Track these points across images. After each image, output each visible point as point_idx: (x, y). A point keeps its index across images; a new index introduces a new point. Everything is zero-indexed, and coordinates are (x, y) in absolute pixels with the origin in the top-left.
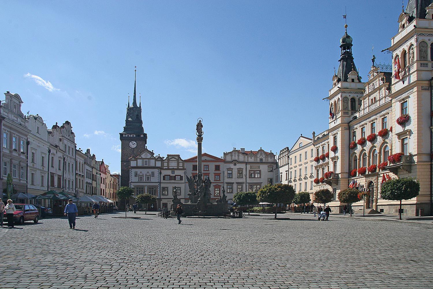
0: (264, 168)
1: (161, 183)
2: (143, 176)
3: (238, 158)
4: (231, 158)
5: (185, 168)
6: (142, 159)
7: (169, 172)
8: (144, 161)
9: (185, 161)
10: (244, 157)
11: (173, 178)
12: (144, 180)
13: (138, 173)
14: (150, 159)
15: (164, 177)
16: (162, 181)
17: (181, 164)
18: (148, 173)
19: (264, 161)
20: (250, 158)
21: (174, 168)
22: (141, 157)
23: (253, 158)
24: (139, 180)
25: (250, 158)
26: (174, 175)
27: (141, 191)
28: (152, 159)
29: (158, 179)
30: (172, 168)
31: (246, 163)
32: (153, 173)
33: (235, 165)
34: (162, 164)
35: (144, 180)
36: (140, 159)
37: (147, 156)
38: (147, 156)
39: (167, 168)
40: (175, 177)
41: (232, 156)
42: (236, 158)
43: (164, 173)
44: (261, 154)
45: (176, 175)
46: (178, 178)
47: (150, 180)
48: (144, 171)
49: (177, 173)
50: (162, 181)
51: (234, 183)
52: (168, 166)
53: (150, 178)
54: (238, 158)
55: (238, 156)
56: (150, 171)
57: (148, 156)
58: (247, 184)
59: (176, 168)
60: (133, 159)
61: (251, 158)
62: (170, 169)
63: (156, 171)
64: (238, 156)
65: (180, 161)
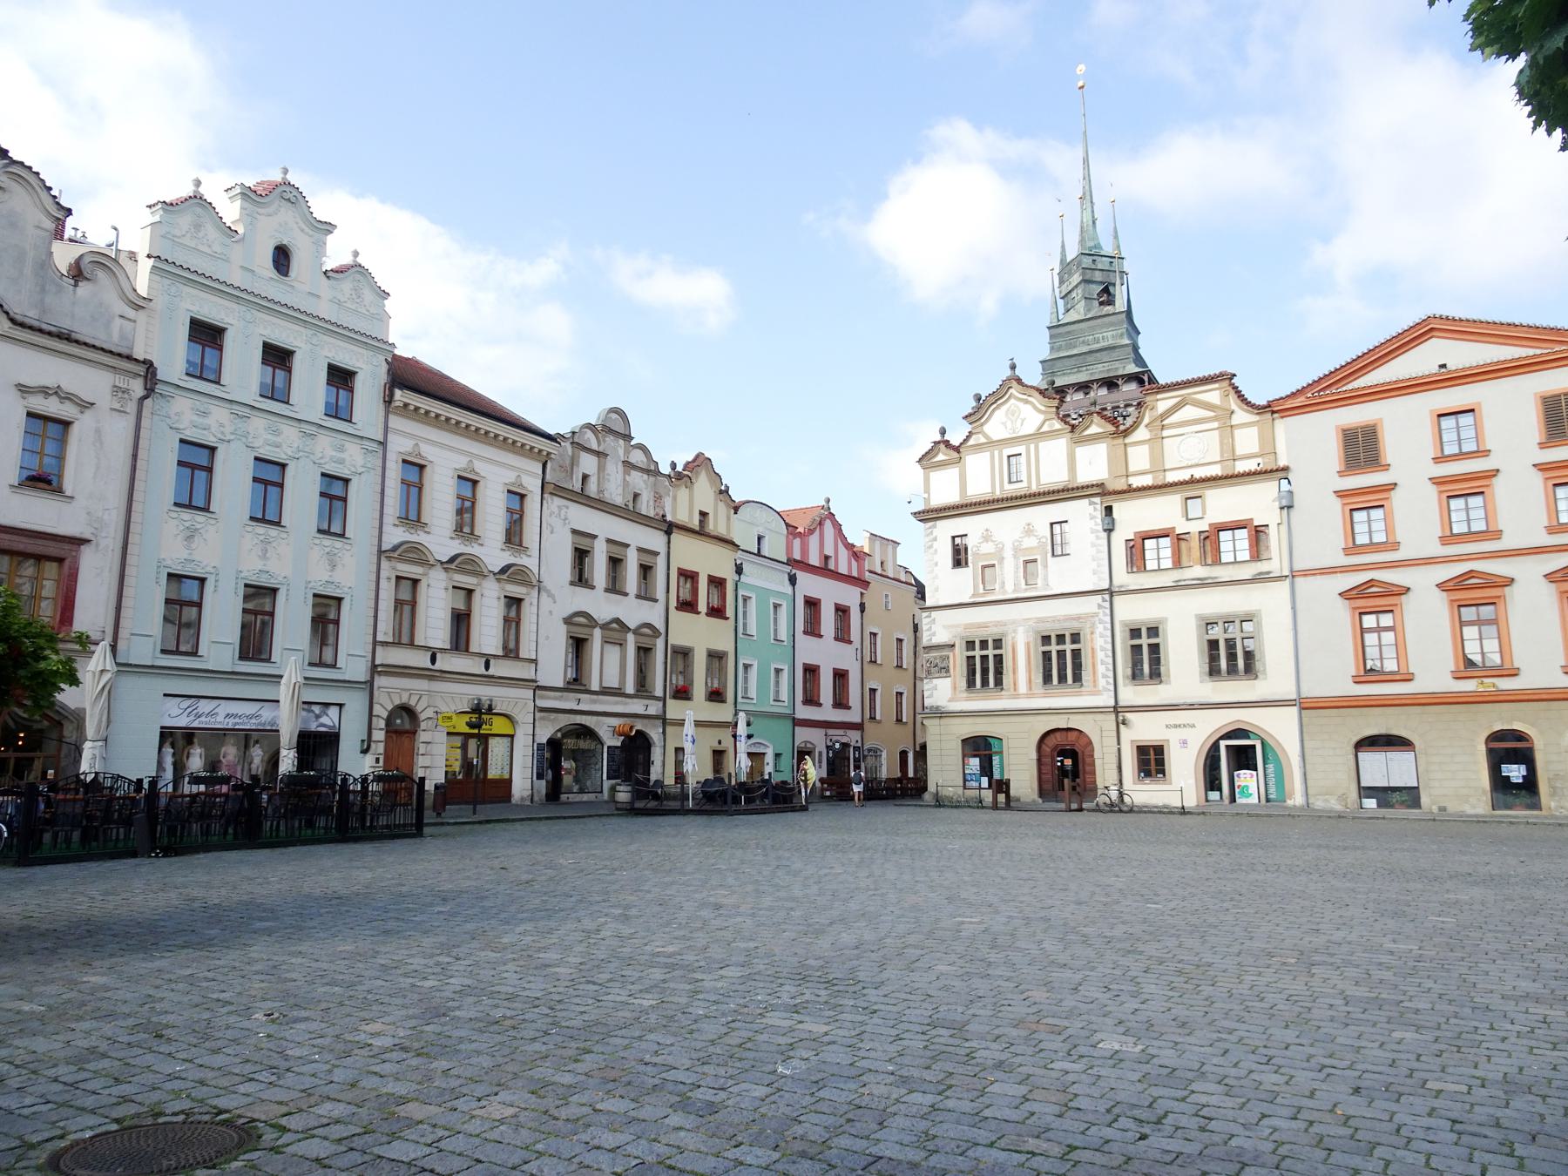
2: (1002, 559)
5: (1282, 464)
6: (991, 444)
7: (1163, 512)
8: (1005, 459)
9: (1271, 409)
12: (1009, 587)
13: (971, 542)
16: (1122, 577)
17: (1248, 440)
18: (1029, 531)
21: (1199, 473)
22: (986, 436)
24: (976, 587)
27: (1145, 650)
28: (1052, 434)
30: (1184, 475)
34: (1120, 462)
35: (1009, 587)
36: (979, 447)
37: (1019, 421)
39: (1147, 480)
40: (1211, 538)
43: (1133, 516)
46: (1235, 545)
47: (1046, 578)
48: (1006, 528)
49: (1222, 505)
50: (1122, 577)
52: (1158, 467)
53: (1046, 566)
56: (1041, 516)
60: (941, 457)
63: (1082, 516)
65: (1241, 416)
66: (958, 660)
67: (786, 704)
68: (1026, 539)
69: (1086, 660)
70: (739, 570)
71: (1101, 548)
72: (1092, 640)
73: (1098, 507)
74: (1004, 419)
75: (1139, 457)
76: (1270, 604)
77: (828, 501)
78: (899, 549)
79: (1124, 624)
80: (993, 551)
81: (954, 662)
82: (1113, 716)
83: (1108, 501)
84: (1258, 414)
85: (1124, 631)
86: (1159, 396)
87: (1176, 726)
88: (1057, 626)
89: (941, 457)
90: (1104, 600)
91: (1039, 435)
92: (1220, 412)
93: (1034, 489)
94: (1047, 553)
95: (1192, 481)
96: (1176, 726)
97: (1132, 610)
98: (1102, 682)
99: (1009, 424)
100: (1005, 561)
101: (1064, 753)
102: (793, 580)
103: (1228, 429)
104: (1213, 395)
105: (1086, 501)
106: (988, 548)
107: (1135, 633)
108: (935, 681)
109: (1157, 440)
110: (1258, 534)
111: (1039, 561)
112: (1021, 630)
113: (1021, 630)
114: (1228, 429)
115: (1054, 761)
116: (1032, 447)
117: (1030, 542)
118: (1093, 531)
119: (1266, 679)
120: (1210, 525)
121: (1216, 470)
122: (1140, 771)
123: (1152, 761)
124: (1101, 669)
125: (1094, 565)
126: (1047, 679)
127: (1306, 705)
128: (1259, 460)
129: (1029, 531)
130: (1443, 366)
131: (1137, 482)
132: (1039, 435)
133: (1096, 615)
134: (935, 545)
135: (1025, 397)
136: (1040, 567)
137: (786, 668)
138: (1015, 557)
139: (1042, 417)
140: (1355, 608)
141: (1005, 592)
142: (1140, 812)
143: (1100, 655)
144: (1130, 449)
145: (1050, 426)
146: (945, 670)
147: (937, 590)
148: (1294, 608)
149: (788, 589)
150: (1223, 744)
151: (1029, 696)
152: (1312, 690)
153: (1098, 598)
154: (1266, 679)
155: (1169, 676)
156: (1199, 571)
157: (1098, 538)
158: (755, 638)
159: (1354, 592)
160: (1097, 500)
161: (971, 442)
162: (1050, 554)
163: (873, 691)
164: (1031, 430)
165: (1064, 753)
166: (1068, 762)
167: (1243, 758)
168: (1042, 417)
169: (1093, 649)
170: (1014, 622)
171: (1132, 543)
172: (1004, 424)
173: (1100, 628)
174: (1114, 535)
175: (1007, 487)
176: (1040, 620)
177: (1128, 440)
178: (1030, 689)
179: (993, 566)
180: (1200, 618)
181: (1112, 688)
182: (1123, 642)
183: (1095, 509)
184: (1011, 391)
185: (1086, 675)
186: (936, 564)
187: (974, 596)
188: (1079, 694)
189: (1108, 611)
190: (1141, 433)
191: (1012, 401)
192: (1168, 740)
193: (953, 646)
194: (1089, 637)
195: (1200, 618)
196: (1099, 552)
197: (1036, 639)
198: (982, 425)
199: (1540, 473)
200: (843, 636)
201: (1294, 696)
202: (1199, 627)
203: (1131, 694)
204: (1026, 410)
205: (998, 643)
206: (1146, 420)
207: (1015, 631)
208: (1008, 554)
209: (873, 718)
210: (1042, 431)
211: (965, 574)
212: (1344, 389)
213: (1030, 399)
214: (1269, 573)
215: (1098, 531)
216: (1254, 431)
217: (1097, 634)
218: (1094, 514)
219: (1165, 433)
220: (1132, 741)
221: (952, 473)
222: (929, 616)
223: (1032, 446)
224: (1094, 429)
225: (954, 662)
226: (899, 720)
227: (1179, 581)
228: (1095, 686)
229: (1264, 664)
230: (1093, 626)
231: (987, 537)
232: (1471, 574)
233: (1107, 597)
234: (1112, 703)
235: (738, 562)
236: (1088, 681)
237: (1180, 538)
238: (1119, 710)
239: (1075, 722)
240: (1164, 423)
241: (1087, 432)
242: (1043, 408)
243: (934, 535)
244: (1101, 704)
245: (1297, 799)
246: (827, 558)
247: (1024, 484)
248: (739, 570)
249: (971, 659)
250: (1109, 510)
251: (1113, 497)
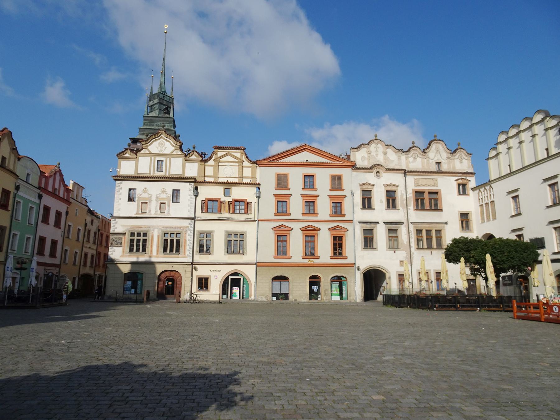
1: (195, 219)
2: (151, 201)
5: (258, 182)
6: (150, 154)
7: (216, 192)
13: (138, 192)
15: (203, 203)
16: (199, 214)
17: (247, 171)
18: (164, 191)
21: (230, 180)
22: (149, 150)
26: (230, 199)
28: (177, 156)
29: (189, 208)
30: (225, 180)
32: (176, 192)
36: (145, 155)
37: (164, 148)
38: (164, 148)
39: (212, 180)
43: (206, 192)
45: (236, 201)
47: (169, 211)
48: (154, 188)
49: (237, 193)
50: (199, 214)
53: (169, 206)
56: (170, 187)
57: (165, 148)
60: (127, 155)
62: (219, 183)
63: (186, 189)
65: (246, 163)
66: (126, 240)
67: (29, 254)
68: (162, 194)
69: (148, 243)
70: (17, 188)
71: (192, 202)
72: (185, 236)
73: (193, 186)
74: (158, 146)
75: (209, 171)
76: (250, 229)
77: (59, 164)
78: (84, 190)
79: (198, 231)
80: (147, 197)
81: (125, 240)
82: (191, 266)
83: (197, 185)
84: (252, 164)
85: (198, 234)
86: (219, 150)
87: (214, 271)
88: (171, 230)
89: (127, 155)
90: (191, 222)
91: (171, 155)
92: (239, 160)
93: (167, 175)
94: (170, 201)
95: (228, 183)
96: (214, 271)
97: (201, 226)
98: (187, 253)
99: (159, 148)
100: (152, 202)
101: (169, 280)
102: (40, 197)
103: (241, 167)
104: (237, 154)
105: (188, 183)
106: (145, 195)
107: (201, 234)
108: (114, 248)
109: (217, 166)
110: (248, 204)
111: (167, 204)
112: (156, 230)
113: (156, 230)
114: (241, 167)
115: (164, 283)
116: (168, 159)
117: (164, 196)
118: (190, 195)
119: (246, 255)
120: (233, 199)
121: (236, 180)
122: (199, 287)
123: (203, 283)
124: (188, 248)
125: (189, 208)
126: (165, 250)
127: (258, 265)
128: (251, 179)
129: (164, 191)
130: (307, 160)
131: (208, 180)
132: (171, 155)
133: (188, 227)
134: (121, 191)
135: (167, 139)
136: (167, 206)
137: (32, 237)
138: (157, 200)
139: (173, 148)
140: (276, 233)
141: (151, 214)
142: (203, 303)
143: (188, 242)
144: (206, 167)
145: (176, 152)
146: (120, 244)
147: (119, 210)
148: (258, 231)
149: (37, 201)
150: (230, 277)
151: (156, 257)
152: (261, 260)
153: (189, 221)
154: (246, 255)
155: (213, 252)
156: (227, 215)
157: (191, 198)
158: (20, 222)
159: (277, 228)
160: (193, 184)
161: (142, 152)
162: (171, 202)
163: (66, 250)
164: (169, 153)
165: (169, 280)
166: (170, 283)
167: (236, 283)
168: (173, 148)
169: (185, 240)
170: (153, 227)
171: (204, 202)
172: (157, 148)
173: (189, 232)
174: (197, 198)
175: (156, 172)
176: (164, 227)
177: (205, 164)
178: (158, 254)
179: (146, 203)
180: (226, 232)
181: (191, 255)
182: (197, 238)
183: (191, 187)
184: (162, 135)
185: (181, 250)
186: (120, 199)
187: (136, 214)
188: (178, 257)
189: (193, 226)
190: (211, 162)
191: (162, 139)
192: (210, 276)
193: (125, 234)
194: (184, 235)
195: (226, 232)
196: (191, 203)
197: (162, 234)
198: (148, 146)
199: (329, 198)
200: (57, 224)
201: (255, 262)
202: (225, 235)
203: (198, 258)
204: (167, 144)
205: (145, 234)
206: (214, 158)
207: (153, 230)
208: (154, 199)
209: (65, 262)
210: (173, 153)
212: (279, 161)
213: (169, 140)
214: (250, 218)
215: (192, 196)
216: (250, 169)
217: (187, 235)
218: (191, 189)
219: (220, 164)
220: (197, 276)
221: (133, 163)
222: (115, 221)
223: (168, 159)
224: (193, 157)
225: (125, 240)
226: (74, 264)
227: (220, 218)
228: (184, 254)
229: (246, 250)
230: (186, 231)
231: (145, 191)
232: (282, 226)
233: (193, 221)
234: (191, 261)
235: (17, 184)
236: (182, 252)
237: (222, 202)
238: (193, 264)
239: (175, 268)
240: (220, 160)
241: (190, 158)
242: (174, 145)
243: (121, 187)
244: (186, 261)
245: (253, 298)
246: (56, 189)
247: (163, 173)
248: (17, 188)
249: (132, 241)
250: (196, 188)
251: (199, 184)
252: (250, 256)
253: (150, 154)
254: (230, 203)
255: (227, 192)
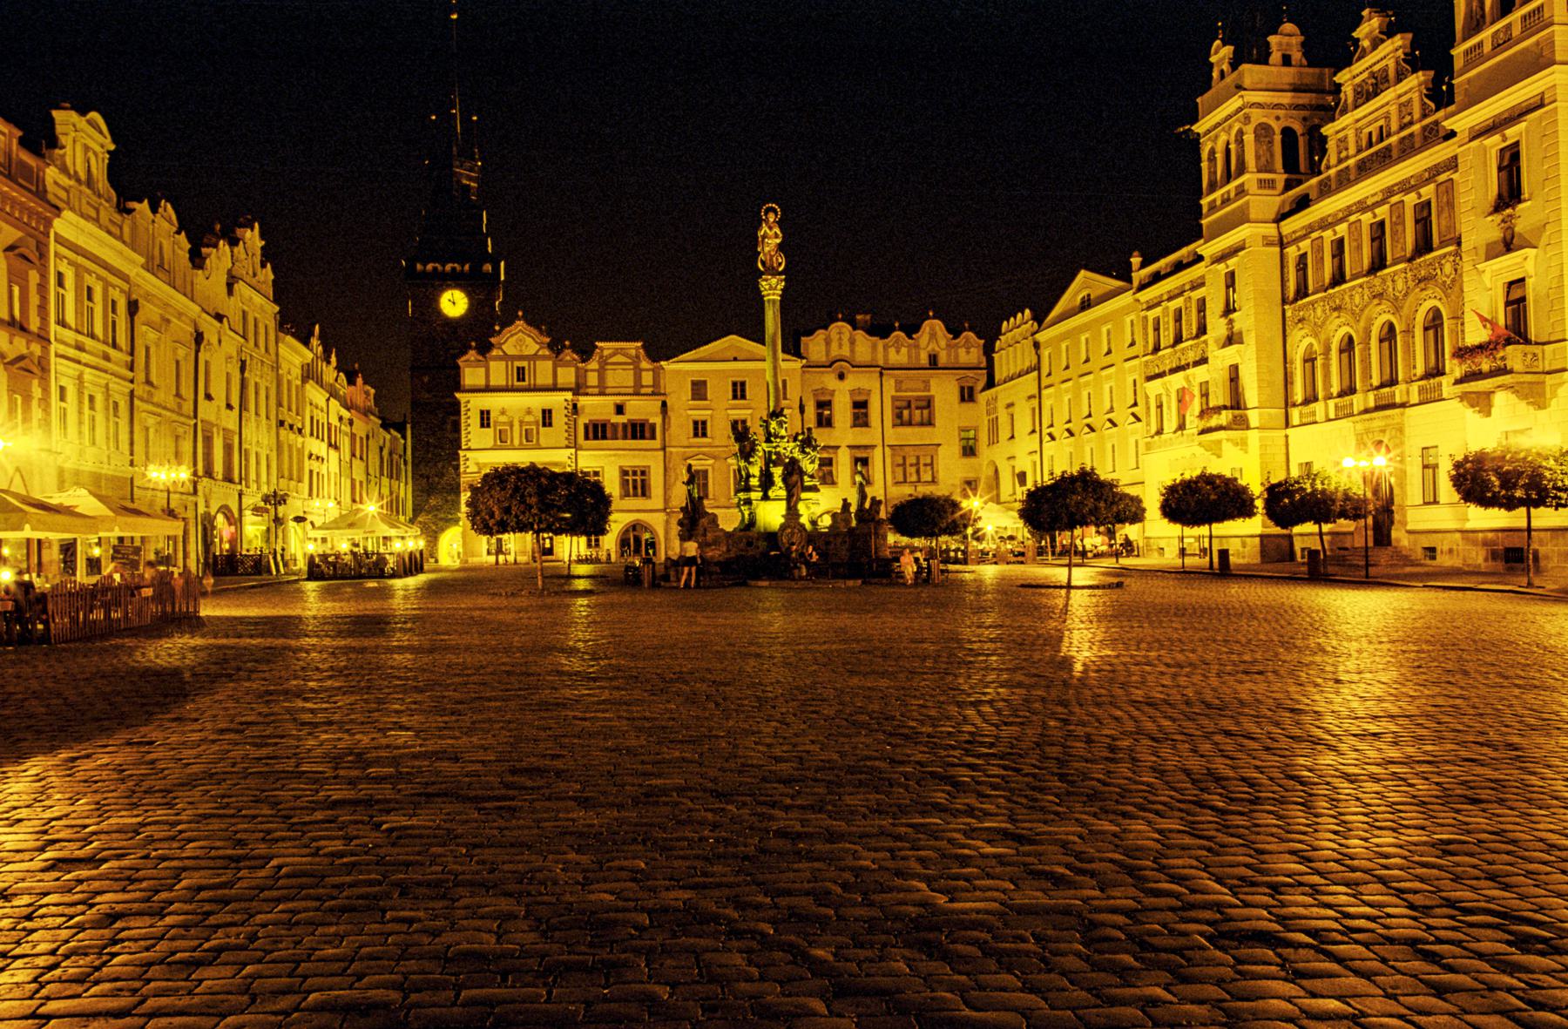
0: (944, 390)
2: (512, 426)
3: (852, 351)
4: (828, 352)
6: (506, 357)
10: (874, 347)
11: (620, 434)
14: (534, 358)
15: (586, 427)
19: (943, 359)
20: (892, 351)
23: (904, 350)
25: (892, 351)
28: (544, 358)
31: (883, 370)
33: (841, 377)
41: (828, 342)
42: (846, 352)
44: (933, 336)
47: (538, 440)
51: (838, 447)
53: (538, 433)
54: (852, 351)
55: (852, 342)
58: (887, 449)
59: (631, 390)
61: (898, 352)
64: (852, 342)
106: (503, 419)
117: (529, 418)
139: (537, 347)
164: (533, 352)
168: (537, 347)
211: (490, 431)
237: (615, 426)
252: (656, 500)
253: (506, 357)
254: (625, 426)
255: (620, 409)
